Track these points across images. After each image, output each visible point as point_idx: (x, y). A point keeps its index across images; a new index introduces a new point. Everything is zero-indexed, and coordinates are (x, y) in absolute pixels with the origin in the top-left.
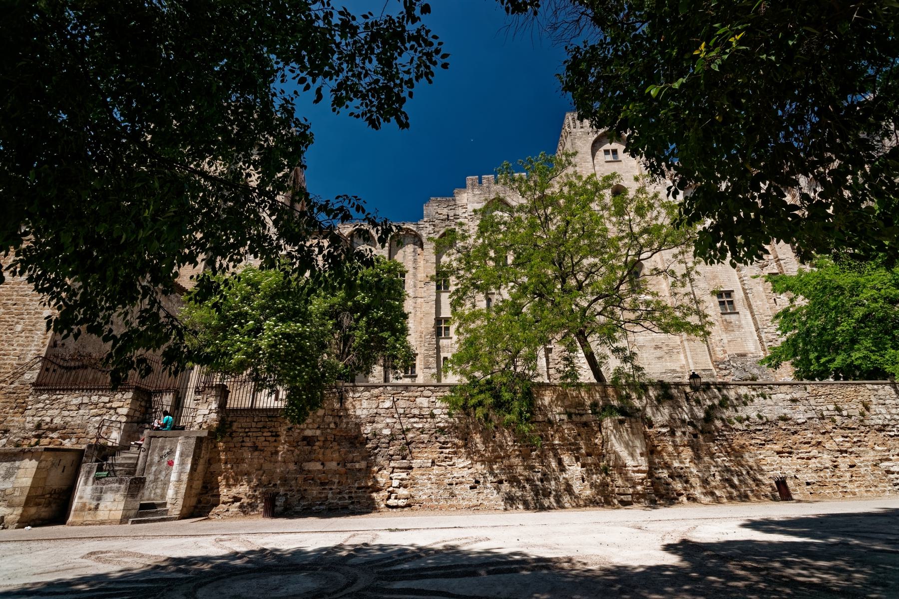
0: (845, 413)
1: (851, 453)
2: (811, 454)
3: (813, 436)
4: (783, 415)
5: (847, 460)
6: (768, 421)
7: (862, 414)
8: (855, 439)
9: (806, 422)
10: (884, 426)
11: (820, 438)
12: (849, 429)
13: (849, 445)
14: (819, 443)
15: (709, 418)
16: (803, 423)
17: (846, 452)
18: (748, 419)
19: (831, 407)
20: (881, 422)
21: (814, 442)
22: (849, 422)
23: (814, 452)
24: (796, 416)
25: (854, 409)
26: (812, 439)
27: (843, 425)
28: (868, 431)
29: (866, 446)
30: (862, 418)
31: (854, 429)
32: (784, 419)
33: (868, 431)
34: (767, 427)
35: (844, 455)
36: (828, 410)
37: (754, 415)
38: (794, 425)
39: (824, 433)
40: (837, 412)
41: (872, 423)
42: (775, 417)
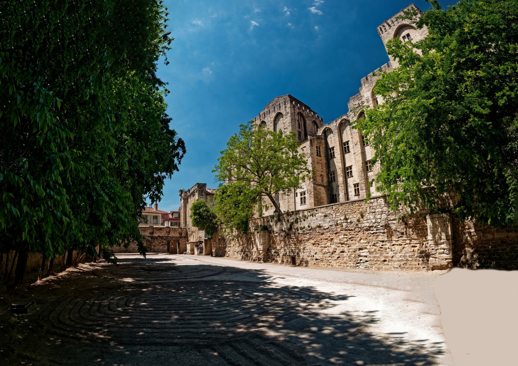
0: (349, 221)
1: (346, 244)
2: (327, 245)
3: (330, 235)
4: (319, 225)
5: (342, 248)
6: (312, 228)
7: (359, 221)
8: (350, 237)
9: (329, 228)
10: (370, 227)
11: (334, 236)
12: (349, 230)
13: (346, 240)
14: (332, 239)
15: (290, 229)
16: (327, 228)
17: (344, 244)
18: (304, 227)
19: (342, 218)
20: (368, 225)
21: (329, 239)
22: (351, 227)
23: (329, 244)
24: (325, 225)
25: (354, 218)
26: (329, 237)
27: (347, 228)
28: (360, 231)
29: (356, 240)
30: (357, 223)
31: (352, 230)
32: (319, 227)
33: (360, 231)
34: (311, 231)
35: (343, 245)
36: (341, 220)
37: (306, 226)
38: (323, 230)
39: (336, 234)
40: (345, 221)
41: (363, 225)
42: (315, 226)
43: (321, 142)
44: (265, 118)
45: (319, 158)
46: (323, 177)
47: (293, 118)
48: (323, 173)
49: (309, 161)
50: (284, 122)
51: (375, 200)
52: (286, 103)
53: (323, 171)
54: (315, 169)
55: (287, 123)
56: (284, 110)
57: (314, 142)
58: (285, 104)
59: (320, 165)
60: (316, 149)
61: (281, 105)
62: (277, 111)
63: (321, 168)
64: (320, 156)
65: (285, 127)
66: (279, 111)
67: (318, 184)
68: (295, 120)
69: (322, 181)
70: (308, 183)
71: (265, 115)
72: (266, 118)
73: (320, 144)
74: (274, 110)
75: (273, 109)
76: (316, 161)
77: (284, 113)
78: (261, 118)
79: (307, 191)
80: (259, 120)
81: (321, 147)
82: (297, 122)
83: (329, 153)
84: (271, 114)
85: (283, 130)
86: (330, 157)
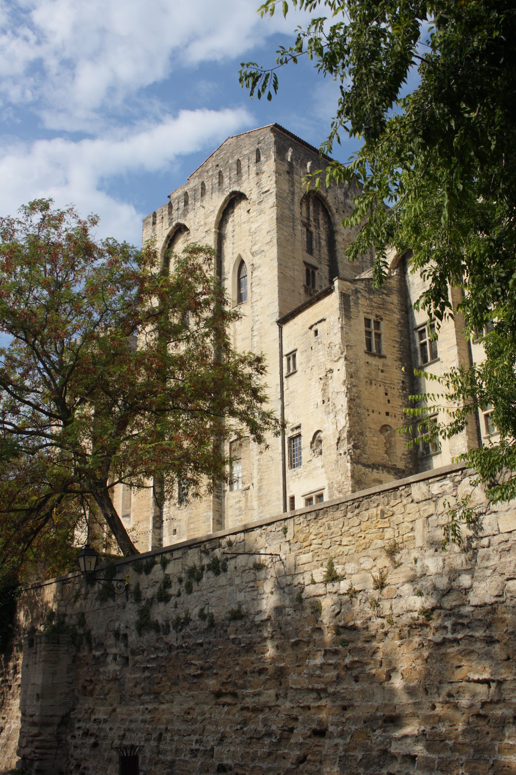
43: (384, 302)
44: (185, 213)
45: (375, 361)
46: (391, 436)
47: (287, 212)
48: (389, 420)
49: (335, 372)
50: (254, 226)
51: (448, 483)
52: (262, 158)
53: (391, 411)
54: (358, 406)
55: (264, 232)
56: (253, 184)
57: (356, 304)
58: (258, 160)
59: (382, 390)
60: (362, 327)
61: (244, 163)
62: (230, 187)
63: (383, 399)
64: (380, 356)
65: (255, 248)
66: (236, 188)
67: (372, 460)
68: (293, 219)
69: (389, 448)
70: (334, 457)
71: (186, 203)
72: (191, 215)
73: (380, 313)
74: (220, 183)
75: (216, 181)
76: (363, 373)
77: (253, 194)
78: (175, 214)
79: (330, 488)
80: (166, 219)
81: (383, 324)
82: (299, 227)
83: (418, 343)
84: (207, 197)
85: (248, 260)
86: (420, 362)
